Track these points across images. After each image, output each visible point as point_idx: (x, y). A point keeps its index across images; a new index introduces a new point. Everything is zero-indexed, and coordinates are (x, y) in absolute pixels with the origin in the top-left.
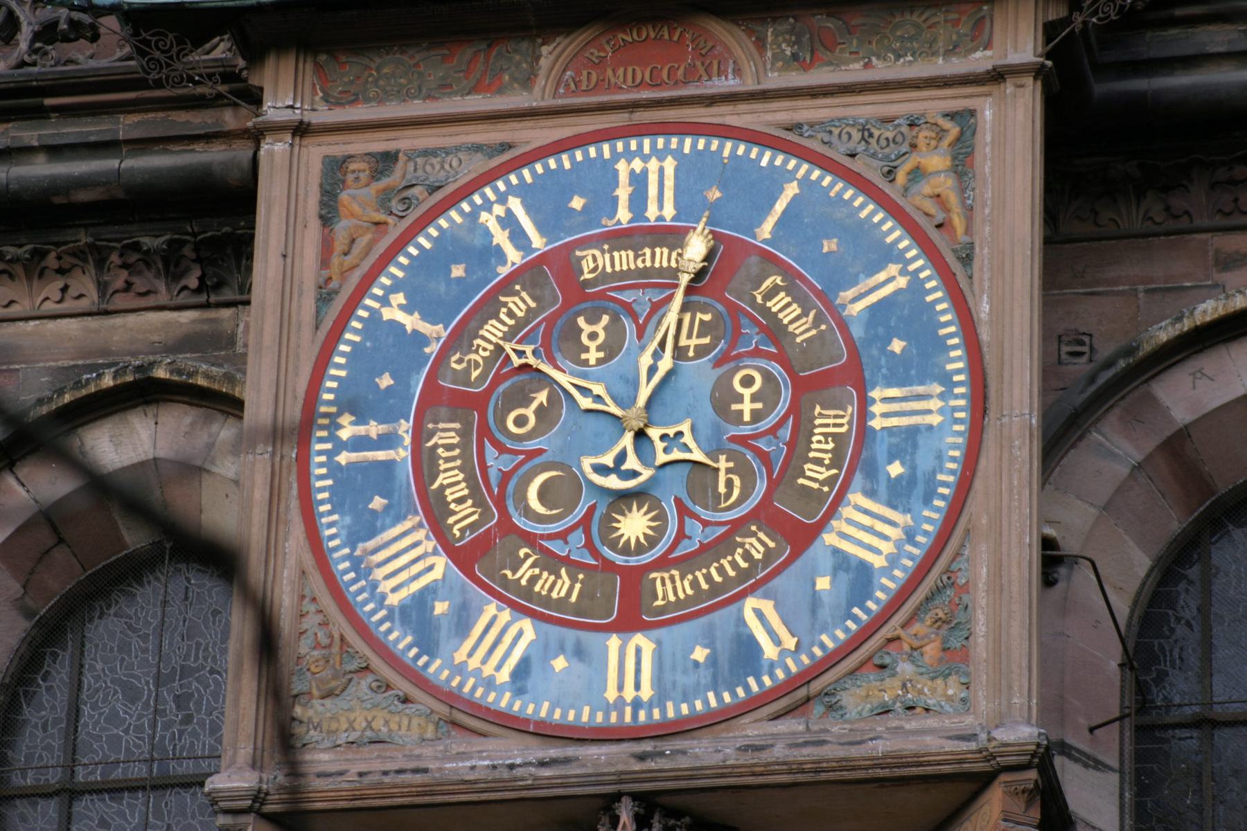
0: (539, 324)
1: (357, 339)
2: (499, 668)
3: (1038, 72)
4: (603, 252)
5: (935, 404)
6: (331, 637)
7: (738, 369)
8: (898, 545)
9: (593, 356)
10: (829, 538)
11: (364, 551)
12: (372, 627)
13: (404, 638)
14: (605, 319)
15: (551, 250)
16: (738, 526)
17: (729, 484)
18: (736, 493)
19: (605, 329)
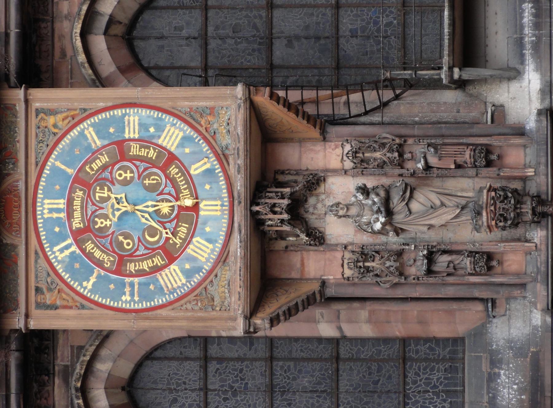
0: (97, 240)
1: (97, 296)
2: (208, 248)
4: (74, 221)
5: (132, 118)
6: (194, 300)
7: (116, 178)
9: (108, 223)
10: (173, 149)
11: (168, 291)
12: (192, 287)
13: (196, 277)
14: (96, 219)
15: (72, 236)
16: (167, 177)
17: (153, 180)
18: (156, 177)
19: (100, 219)
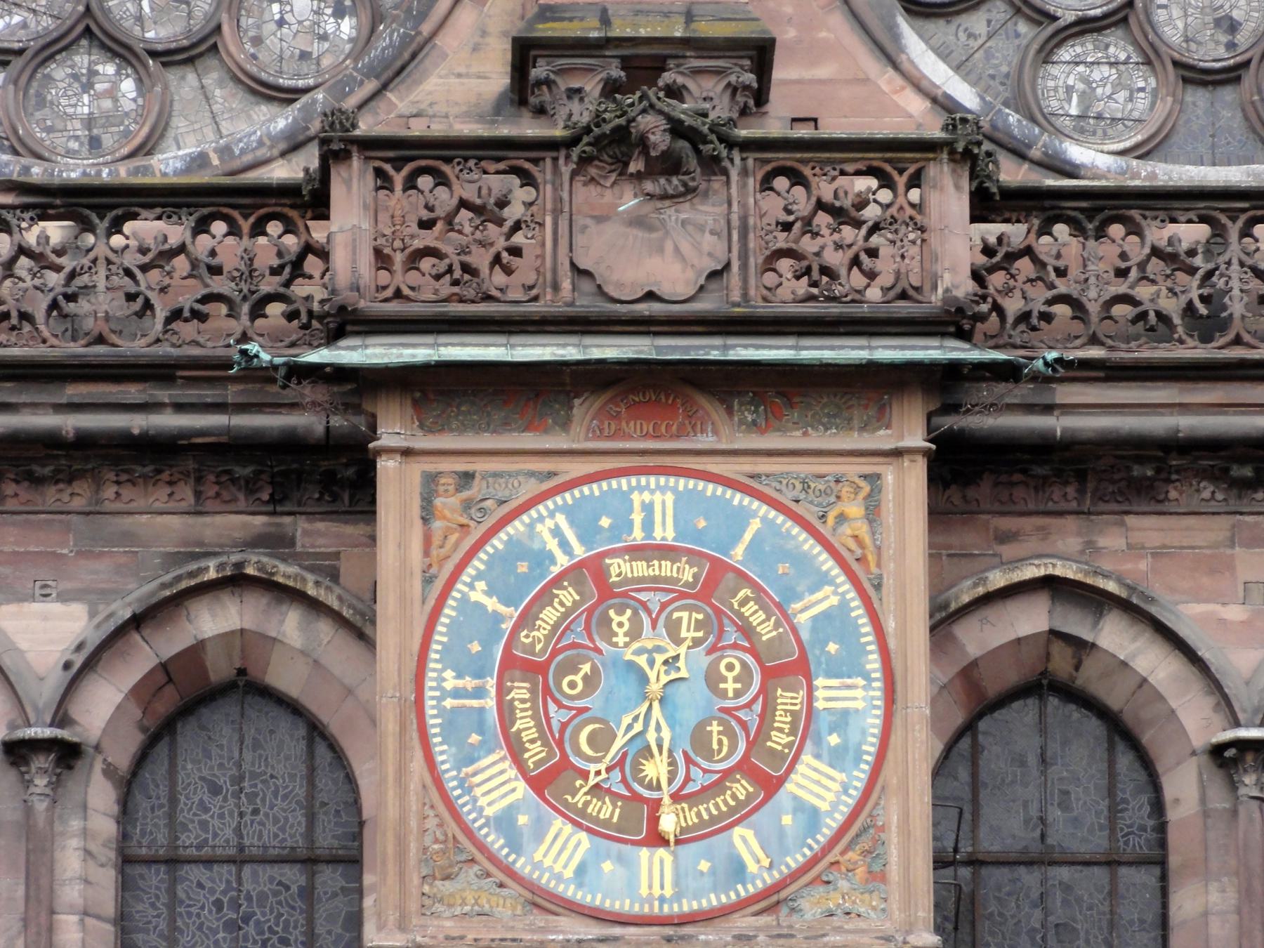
1: (454, 614)
2: (565, 867)
3: (926, 453)
4: (625, 561)
5: (859, 693)
6: (446, 835)
7: (722, 657)
8: (837, 793)
9: (621, 639)
10: (789, 786)
11: (467, 774)
12: (475, 831)
14: (629, 612)
15: (589, 557)
16: (727, 774)
17: (720, 742)
18: (725, 749)
